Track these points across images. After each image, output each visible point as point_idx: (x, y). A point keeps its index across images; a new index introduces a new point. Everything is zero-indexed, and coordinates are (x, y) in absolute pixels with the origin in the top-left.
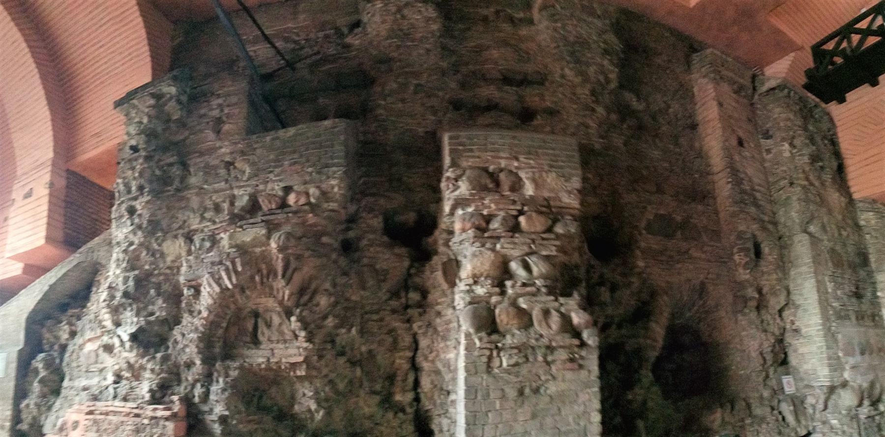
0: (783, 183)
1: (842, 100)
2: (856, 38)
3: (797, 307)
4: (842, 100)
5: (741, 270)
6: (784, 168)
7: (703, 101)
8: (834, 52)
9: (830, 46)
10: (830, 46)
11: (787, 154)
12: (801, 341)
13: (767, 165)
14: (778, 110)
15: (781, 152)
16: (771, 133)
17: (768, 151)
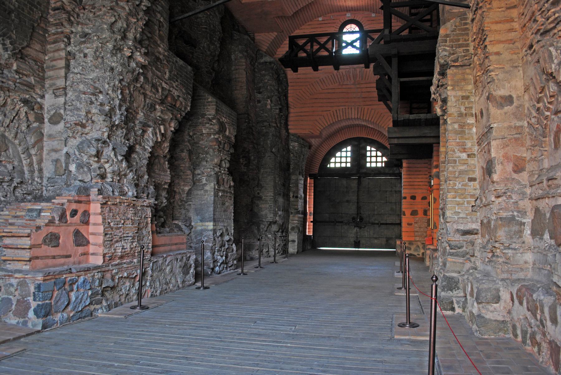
0: (265, 124)
1: (295, 70)
2: (316, 47)
3: (262, 187)
4: (295, 70)
5: (243, 167)
6: (266, 115)
7: (237, 67)
8: (302, 48)
9: (301, 42)
10: (301, 42)
11: (269, 107)
12: (261, 202)
13: (258, 109)
14: (267, 77)
15: (266, 105)
16: (261, 90)
17: (259, 101)
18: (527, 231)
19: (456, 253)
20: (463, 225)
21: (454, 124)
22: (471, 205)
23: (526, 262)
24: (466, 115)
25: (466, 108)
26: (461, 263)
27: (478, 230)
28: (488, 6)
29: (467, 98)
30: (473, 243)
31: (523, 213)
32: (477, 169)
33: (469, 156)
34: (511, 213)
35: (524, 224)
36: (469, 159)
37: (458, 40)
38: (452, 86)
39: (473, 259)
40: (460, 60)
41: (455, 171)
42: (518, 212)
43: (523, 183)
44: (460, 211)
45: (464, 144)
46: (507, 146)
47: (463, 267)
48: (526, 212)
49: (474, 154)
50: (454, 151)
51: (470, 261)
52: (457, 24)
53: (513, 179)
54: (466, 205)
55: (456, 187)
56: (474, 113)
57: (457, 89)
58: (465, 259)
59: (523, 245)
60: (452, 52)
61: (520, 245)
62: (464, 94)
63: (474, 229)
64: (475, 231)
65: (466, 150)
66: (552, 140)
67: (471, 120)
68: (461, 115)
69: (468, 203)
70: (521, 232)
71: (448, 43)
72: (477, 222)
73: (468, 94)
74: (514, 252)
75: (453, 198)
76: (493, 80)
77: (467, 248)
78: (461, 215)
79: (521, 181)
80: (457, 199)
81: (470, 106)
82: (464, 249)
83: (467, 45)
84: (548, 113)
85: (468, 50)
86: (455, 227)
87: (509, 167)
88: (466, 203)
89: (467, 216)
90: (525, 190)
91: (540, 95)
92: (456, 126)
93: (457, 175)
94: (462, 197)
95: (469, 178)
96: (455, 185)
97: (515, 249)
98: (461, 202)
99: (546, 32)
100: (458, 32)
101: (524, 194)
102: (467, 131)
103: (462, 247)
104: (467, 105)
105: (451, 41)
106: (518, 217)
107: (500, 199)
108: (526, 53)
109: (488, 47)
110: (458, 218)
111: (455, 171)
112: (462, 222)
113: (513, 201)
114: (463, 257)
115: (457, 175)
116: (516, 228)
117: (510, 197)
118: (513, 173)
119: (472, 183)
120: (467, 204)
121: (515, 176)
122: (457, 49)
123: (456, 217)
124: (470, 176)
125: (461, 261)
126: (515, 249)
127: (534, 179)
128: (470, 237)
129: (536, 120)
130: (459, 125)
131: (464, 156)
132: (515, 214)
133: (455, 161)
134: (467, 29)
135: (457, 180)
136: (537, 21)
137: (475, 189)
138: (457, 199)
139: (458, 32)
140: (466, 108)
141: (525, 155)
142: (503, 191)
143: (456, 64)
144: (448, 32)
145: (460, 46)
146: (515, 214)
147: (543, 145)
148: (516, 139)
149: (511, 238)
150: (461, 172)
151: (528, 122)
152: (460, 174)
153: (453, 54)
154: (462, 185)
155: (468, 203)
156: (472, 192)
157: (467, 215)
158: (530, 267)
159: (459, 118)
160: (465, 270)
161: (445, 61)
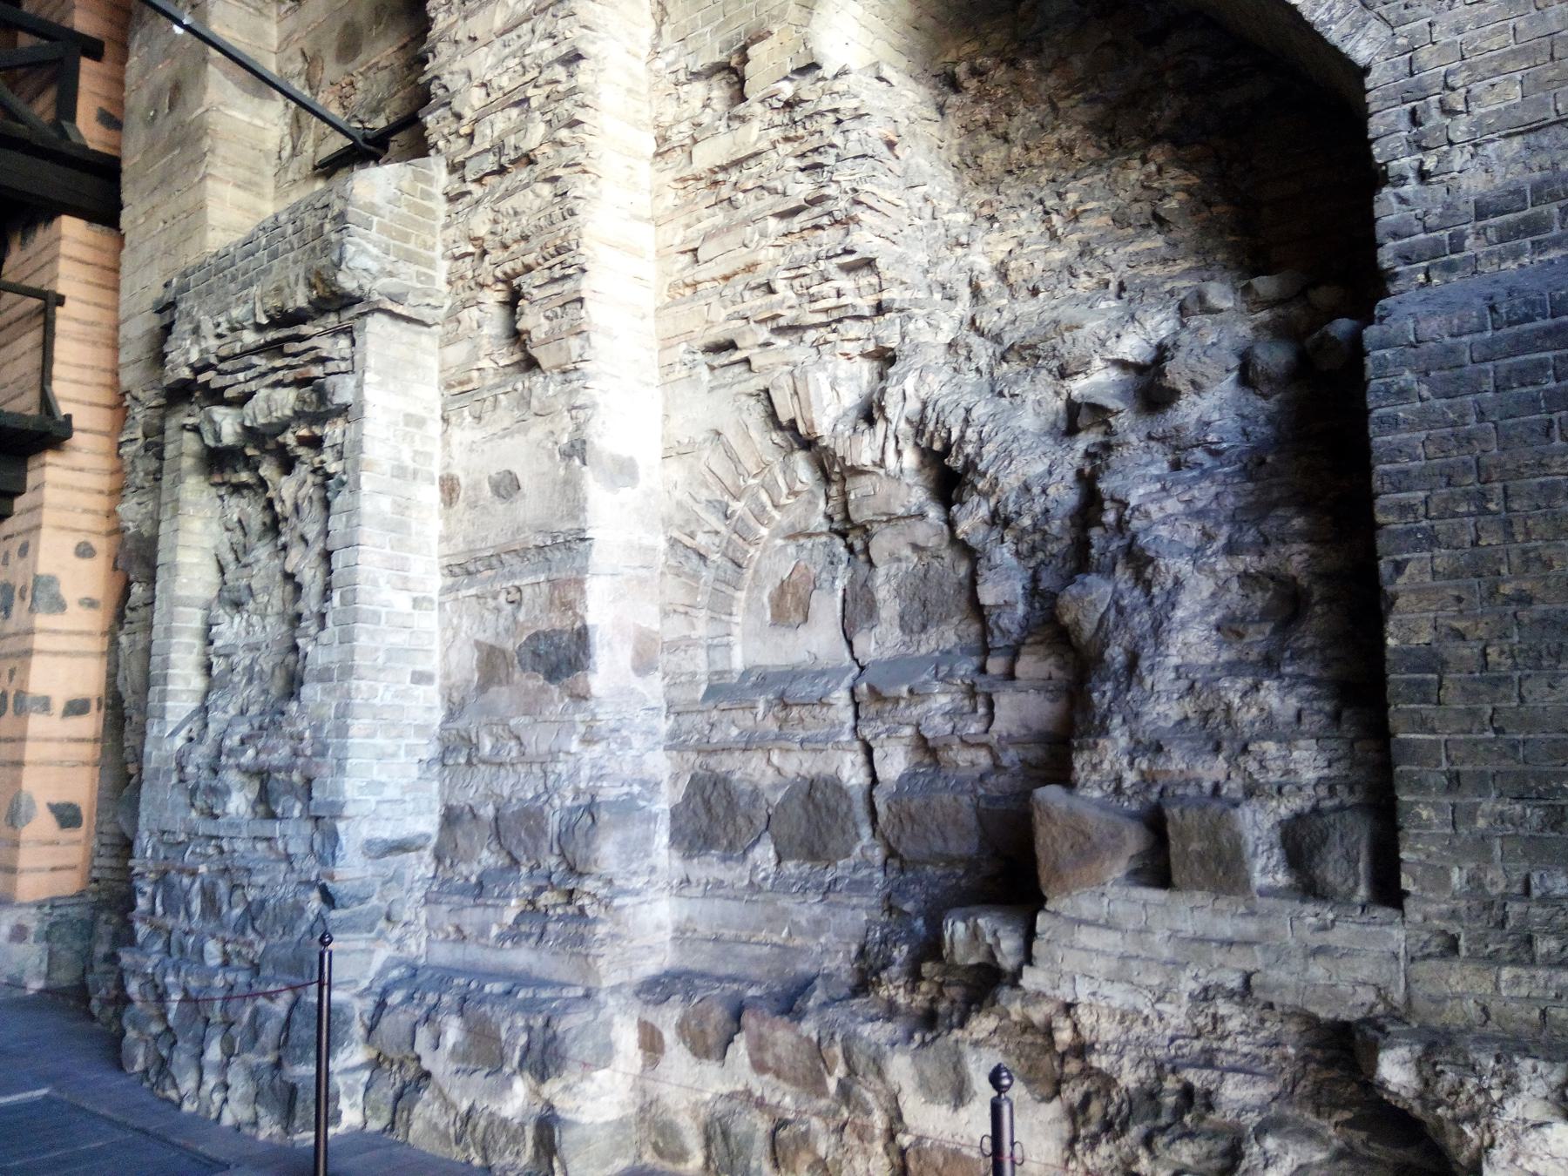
18: (662, 838)
19: (349, 919)
20: (390, 826)
21: (380, 497)
22: (416, 759)
23: (659, 927)
24: (415, 473)
25: (416, 452)
26: (363, 951)
27: (428, 838)
28: (589, 188)
29: (420, 422)
30: (396, 878)
31: (650, 786)
32: (437, 647)
33: (416, 603)
34: (626, 789)
35: (653, 818)
36: (416, 612)
37: (405, 237)
38: (378, 373)
39: (397, 932)
40: (411, 299)
41: (377, 650)
42: (643, 783)
43: (653, 703)
44: (383, 778)
45: (401, 567)
46: (623, 596)
47: (369, 964)
48: (658, 784)
49: (431, 601)
50: (375, 583)
51: (386, 939)
52: (405, 185)
53: (632, 692)
54: (403, 759)
55: (377, 701)
56: (437, 476)
57: (391, 387)
58: (373, 935)
59: (654, 878)
60: (389, 267)
61: (646, 879)
62: (412, 410)
63: (420, 836)
64: (420, 842)
65: (410, 585)
66: (765, 599)
67: (431, 495)
68: (400, 472)
69: (410, 751)
70: (648, 839)
71: (374, 234)
72: (431, 811)
73: (424, 414)
74: (635, 900)
75: (368, 736)
76: (594, 405)
77: (382, 897)
78: (391, 793)
79: (649, 697)
80: (380, 740)
81: (427, 449)
82: (374, 901)
83: (431, 263)
84: (764, 531)
85: (431, 279)
86: (366, 831)
87: (625, 656)
88: (402, 752)
89: (404, 793)
90: (655, 722)
91: (751, 481)
92: (385, 504)
93: (380, 661)
94: (394, 733)
95: (414, 673)
96: (373, 692)
97: (637, 893)
98: (390, 750)
99: (795, 329)
100: (404, 210)
101: (651, 732)
102: (414, 526)
103: (369, 897)
104: (418, 446)
105: (383, 229)
106: (644, 798)
107: (598, 749)
108: (689, 357)
109: (587, 303)
110: (379, 802)
111: (377, 650)
112: (386, 815)
113: (633, 752)
114: (370, 931)
115: (380, 661)
116: (636, 832)
117: (625, 743)
118: (631, 673)
119: (421, 690)
120: (408, 753)
121: (638, 684)
122: (400, 264)
123: (373, 799)
124: (419, 668)
125: (362, 945)
126: (637, 893)
127: (700, 696)
128: (394, 860)
129: (717, 541)
130: (394, 502)
131: (402, 602)
132: (636, 789)
133: (376, 616)
134: (428, 212)
135: (382, 676)
136: (772, 291)
137: (430, 709)
138: (380, 740)
139: (404, 210)
140: (416, 452)
141: (656, 627)
142: (612, 724)
143: (398, 309)
144: (378, 199)
145: (410, 257)
146: (636, 789)
147: (735, 610)
148: (642, 582)
149: (630, 861)
150: (393, 654)
151: (674, 543)
152: (389, 659)
153: (391, 274)
154: (396, 696)
155: (410, 751)
156: (421, 718)
157: (405, 790)
158: (668, 938)
159: (395, 480)
160: (371, 974)
161: (360, 287)
